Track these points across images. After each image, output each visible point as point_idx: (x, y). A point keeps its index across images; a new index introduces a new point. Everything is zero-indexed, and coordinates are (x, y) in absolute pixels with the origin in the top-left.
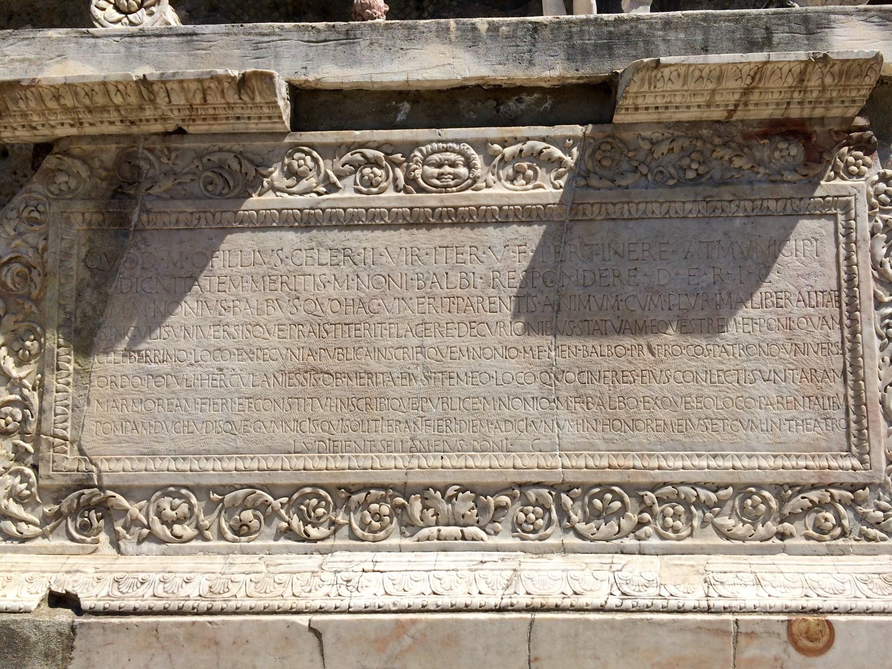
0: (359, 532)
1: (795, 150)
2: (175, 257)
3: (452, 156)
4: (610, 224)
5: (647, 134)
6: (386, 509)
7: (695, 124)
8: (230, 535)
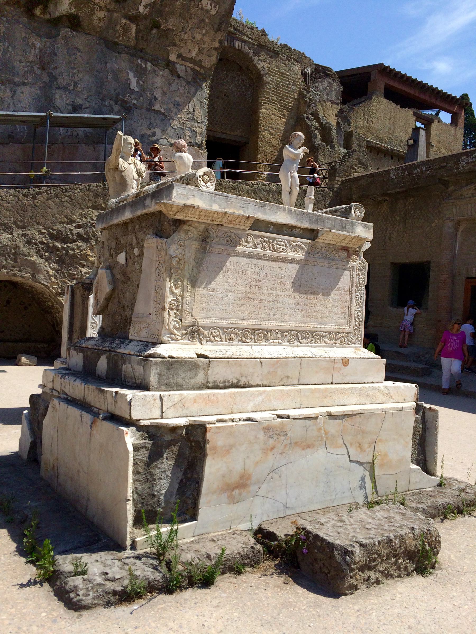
0: (257, 341)
3: (283, 243)
5: (321, 245)
6: (262, 335)
7: (330, 244)
8: (228, 341)
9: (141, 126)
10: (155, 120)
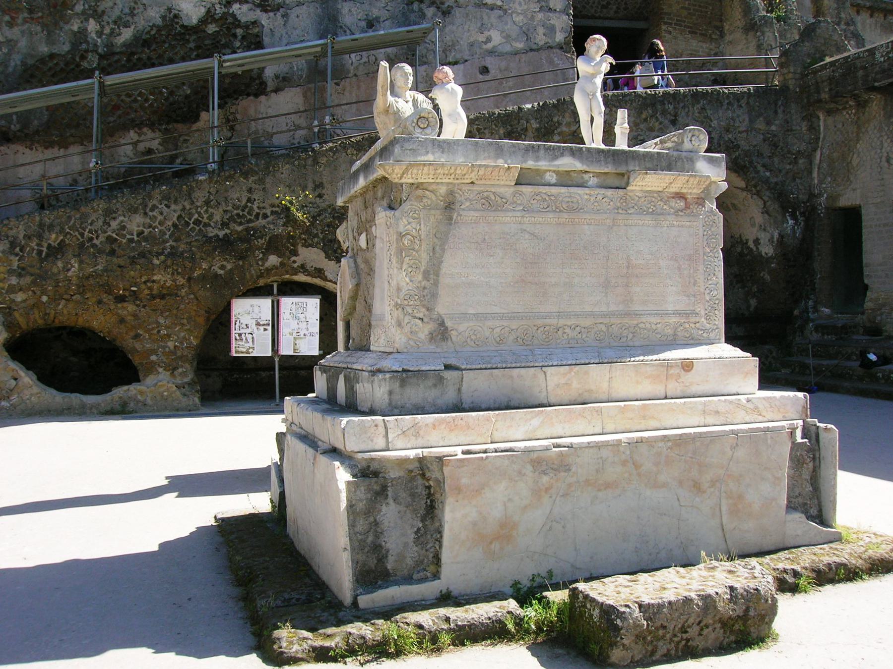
1: (682, 204)
2: (470, 234)
4: (625, 227)
9: (469, 31)
10: (489, 17)
